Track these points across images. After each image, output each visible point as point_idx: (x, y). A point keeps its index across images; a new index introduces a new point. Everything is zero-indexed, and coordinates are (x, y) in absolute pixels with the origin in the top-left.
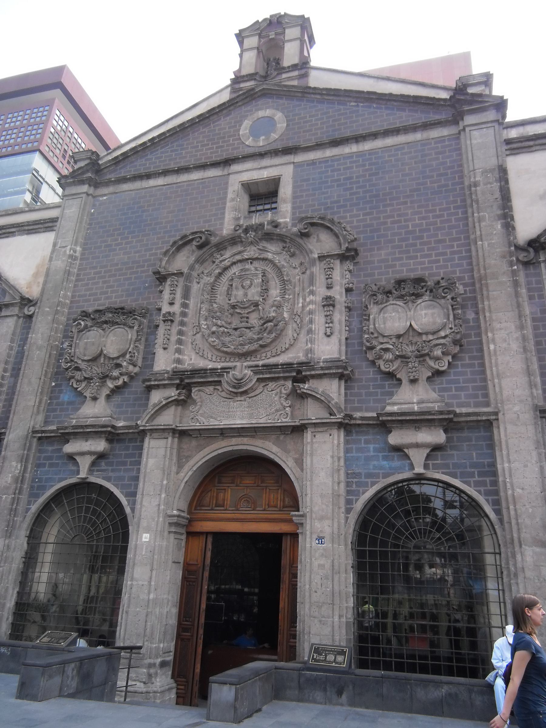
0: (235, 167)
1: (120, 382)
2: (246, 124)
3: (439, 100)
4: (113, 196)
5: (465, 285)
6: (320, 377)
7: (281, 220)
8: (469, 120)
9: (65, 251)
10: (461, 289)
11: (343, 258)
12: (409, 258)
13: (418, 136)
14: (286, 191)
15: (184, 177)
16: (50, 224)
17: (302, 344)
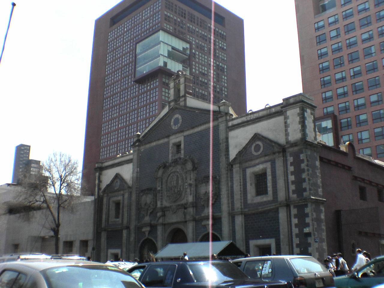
1: (151, 211)
2: (173, 120)
5: (219, 176)
6: (189, 207)
7: (182, 157)
8: (220, 120)
10: (218, 177)
11: (193, 170)
14: (182, 146)
16: (131, 161)
17: (186, 198)
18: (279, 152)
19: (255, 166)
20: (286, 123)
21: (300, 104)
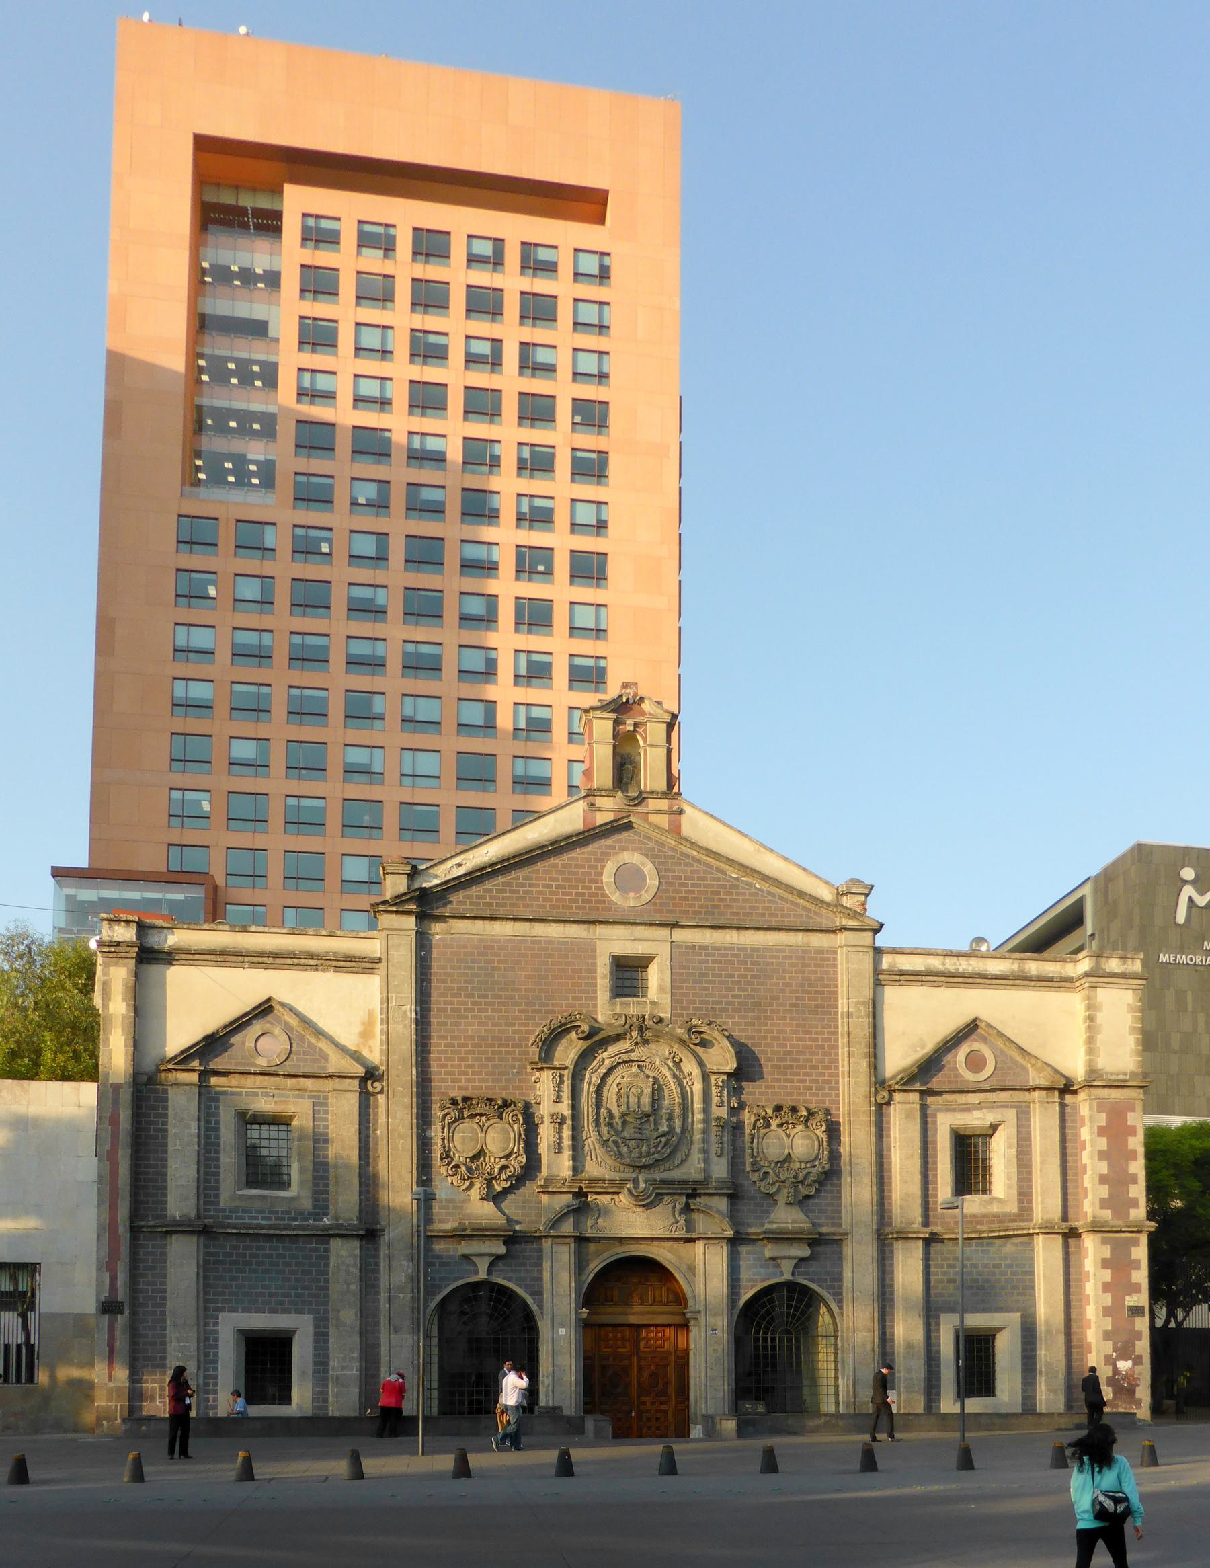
0: (600, 930)
3: (823, 902)
4: (449, 936)
9: (405, 1012)
12: (786, 1081)
13: (798, 939)
15: (539, 930)
18: (1049, 1089)
19: (967, 1109)
20: (1091, 1018)
21: (1140, 982)
